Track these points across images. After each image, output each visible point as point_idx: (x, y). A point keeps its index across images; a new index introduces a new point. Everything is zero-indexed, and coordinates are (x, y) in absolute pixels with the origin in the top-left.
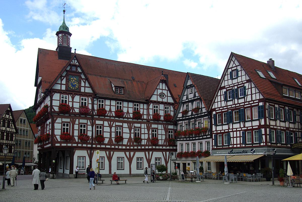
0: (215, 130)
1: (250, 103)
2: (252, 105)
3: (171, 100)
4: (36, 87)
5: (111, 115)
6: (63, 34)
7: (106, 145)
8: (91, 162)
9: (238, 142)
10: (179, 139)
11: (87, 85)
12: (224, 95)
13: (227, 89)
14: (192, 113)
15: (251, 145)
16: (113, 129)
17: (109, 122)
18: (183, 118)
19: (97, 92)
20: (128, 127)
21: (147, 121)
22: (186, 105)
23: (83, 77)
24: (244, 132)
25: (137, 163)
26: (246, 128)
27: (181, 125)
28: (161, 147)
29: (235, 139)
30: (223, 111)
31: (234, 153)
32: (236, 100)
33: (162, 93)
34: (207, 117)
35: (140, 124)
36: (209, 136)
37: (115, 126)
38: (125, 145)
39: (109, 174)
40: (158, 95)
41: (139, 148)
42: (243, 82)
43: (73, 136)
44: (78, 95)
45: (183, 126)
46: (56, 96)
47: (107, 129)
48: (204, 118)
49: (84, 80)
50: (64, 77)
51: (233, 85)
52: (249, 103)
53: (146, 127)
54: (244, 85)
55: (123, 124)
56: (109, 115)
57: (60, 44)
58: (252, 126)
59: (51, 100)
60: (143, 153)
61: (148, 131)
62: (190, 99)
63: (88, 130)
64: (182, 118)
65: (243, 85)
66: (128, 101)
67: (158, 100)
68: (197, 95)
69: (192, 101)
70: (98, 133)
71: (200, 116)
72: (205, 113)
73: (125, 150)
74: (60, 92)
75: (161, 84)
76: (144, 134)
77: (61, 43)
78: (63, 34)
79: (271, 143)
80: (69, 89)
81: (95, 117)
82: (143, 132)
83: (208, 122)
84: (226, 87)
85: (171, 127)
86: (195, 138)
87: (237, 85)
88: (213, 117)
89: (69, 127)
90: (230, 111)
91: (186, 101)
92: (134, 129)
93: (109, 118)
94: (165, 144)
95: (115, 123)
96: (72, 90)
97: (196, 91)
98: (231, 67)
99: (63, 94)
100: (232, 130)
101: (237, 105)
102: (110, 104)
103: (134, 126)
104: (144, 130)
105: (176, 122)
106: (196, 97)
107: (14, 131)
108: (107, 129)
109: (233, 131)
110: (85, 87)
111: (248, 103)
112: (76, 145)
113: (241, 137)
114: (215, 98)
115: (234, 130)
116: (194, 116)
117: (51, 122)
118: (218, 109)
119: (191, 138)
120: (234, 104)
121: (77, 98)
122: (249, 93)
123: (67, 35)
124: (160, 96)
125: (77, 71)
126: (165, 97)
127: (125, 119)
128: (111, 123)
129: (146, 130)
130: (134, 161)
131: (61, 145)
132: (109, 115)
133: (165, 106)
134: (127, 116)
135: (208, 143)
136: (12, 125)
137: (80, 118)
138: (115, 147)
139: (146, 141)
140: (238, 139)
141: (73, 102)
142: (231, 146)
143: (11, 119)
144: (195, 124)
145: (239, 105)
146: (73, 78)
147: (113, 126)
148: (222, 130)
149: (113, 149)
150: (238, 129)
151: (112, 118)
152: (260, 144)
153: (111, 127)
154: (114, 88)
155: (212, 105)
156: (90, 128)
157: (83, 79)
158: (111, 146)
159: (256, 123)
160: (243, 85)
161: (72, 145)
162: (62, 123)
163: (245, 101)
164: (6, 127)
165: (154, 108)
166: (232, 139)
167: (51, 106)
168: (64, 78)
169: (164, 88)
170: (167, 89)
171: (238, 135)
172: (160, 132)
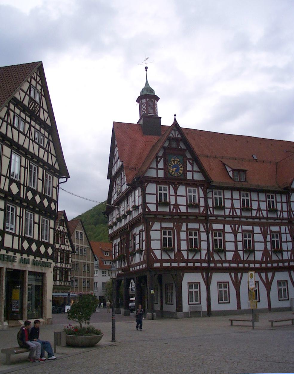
4: (110, 180)
5: (235, 214)
6: (148, 99)
7: (229, 262)
11: (196, 168)
16: (239, 237)
17: (233, 226)
19: (213, 180)
20: (261, 232)
21: (289, 221)
23: (189, 156)
25: (280, 291)
35: (279, 227)
37: (241, 231)
38: (258, 262)
39: (237, 309)
41: (281, 264)
43: (179, 250)
44: (182, 185)
46: (151, 188)
49: (191, 161)
50: (161, 157)
53: (288, 231)
55: (253, 228)
57: (144, 113)
60: (287, 273)
63: (186, 241)
74: (156, 181)
76: (287, 242)
77: (145, 112)
78: (148, 99)
80: (169, 176)
81: (210, 218)
82: (284, 239)
89: (171, 236)
93: (231, 219)
95: (241, 226)
99: (160, 184)
102: (232, 197)
103: (271, 231)
107: (71, 249)
108: (230, 237)
112: (183, 264)
117: (143, 229)
121: (182, 190)
123: (153, 100)
125: (180, 148)
127: (256, 220)
130: (274, 287)
134: (258, 215)
136: (67, 241)
139: (290, 253)
141: (176, 196)
143: (65, 233)
147: (239, 231)
149: (241, 268)
151: (236, 219)
153: (235, 233)
154: (231, 174)
156: (204, 236)
157: (189, 160)
158: (238, 265)
164: (60, 244)
168: (160, 160)
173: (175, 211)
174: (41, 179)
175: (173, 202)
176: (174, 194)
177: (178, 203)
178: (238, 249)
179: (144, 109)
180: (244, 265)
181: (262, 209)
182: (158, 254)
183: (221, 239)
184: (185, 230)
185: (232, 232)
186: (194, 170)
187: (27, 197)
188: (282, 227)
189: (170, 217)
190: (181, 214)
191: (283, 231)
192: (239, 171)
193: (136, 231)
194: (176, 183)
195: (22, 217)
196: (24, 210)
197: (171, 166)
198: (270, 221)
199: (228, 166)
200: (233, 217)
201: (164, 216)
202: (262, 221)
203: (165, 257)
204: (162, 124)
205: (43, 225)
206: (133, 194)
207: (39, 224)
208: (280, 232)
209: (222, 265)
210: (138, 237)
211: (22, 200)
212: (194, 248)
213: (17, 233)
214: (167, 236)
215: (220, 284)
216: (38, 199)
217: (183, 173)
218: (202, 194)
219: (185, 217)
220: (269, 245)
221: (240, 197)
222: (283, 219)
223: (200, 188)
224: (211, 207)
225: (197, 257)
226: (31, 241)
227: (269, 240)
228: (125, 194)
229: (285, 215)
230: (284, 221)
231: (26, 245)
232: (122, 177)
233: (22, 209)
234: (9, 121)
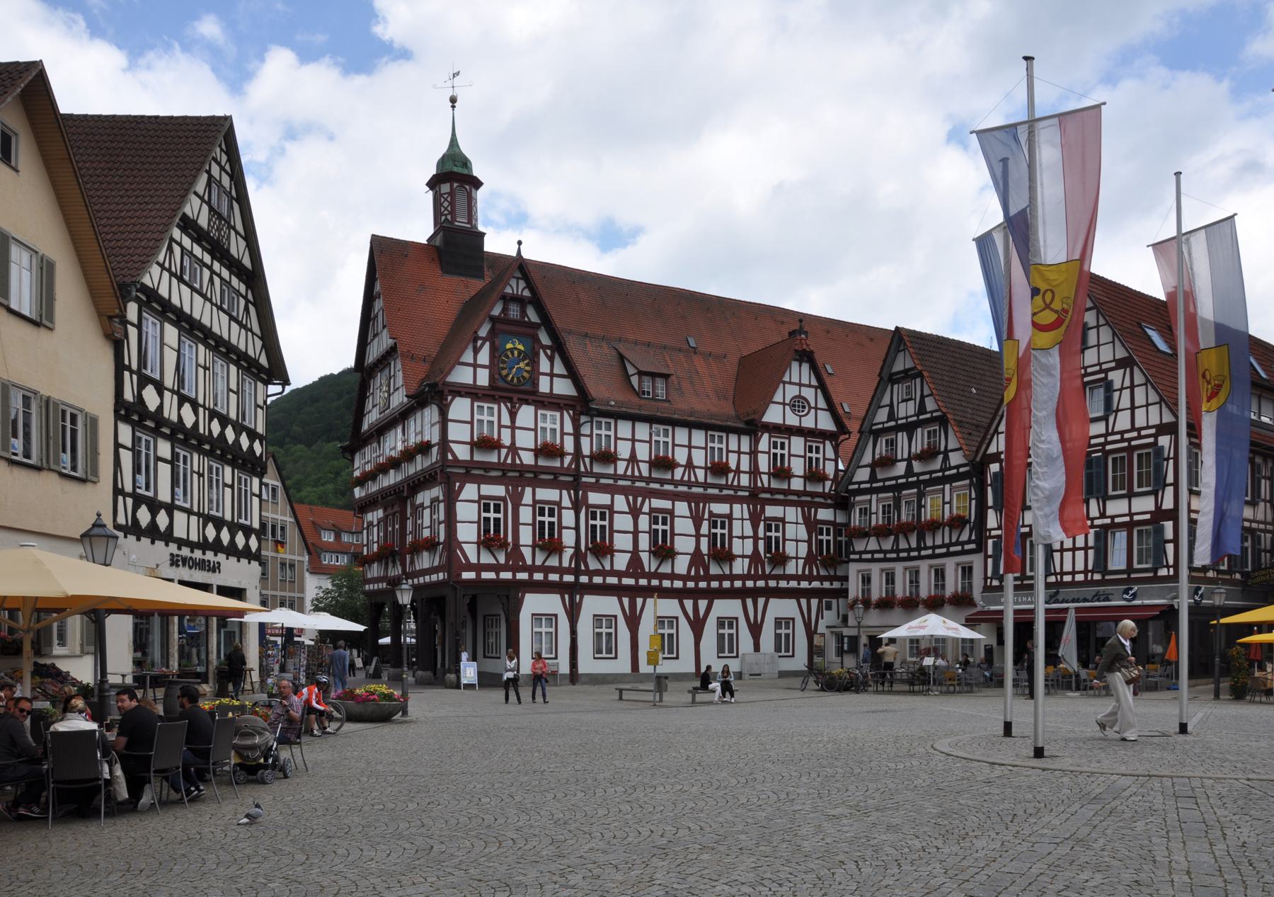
0: (996, 526)
3: (826, 423)
5: (637, 473)
9: (1080, 566)
10: (857, 557)
11: (559, 368)
14: (909, 467)
15: (1125, 576)
16: (644, 522)
17: (631, 498)
18: (874, 485)
19: (594, 397)
22: (887, 441)
24: (1103, 534)
25: (721, 638)
26: (1108, 521)
27: (866, 509)
28: (793, 584)
29: (1068, 555)
33: (800, 396)
34: (967, 482)
35: (728, 506)
38: (679, 577)
39: (630, 672)
40: (787, 404)
41: (726, 584)
43: (517, 545)
44: (528, 404)
45: (874, 510)
46: (460, 408)
47: (623, 522)
48: (954, 484)
53: (746, 515)
56: (629, 473)
58: (1131, 514)
59: (444, 422)
60: (738, 602)
61: (755, 527)
62: (904, 421)
64: (868, 485)
65: (1103, 375)
66: (691, 425)
67: (786, 423)
68: (930, 404)
69: (910, 428)
70: (594, 537)
71: (938, 477)
72: (957, 467)
74: (473, 393)
75: (795, 365)
76: (743, 538)
79: (1219, 572)
80: (501, 384)
81: (584, 479)
82: (737, 531)
83: (971, 499)
85: (824, 514)
88: (989, 482)
89: (501, 516)
91: (886, 425)
92: (709, 520)
93: (629, 483)
94: (807, 572)
95: (647, 500)
96: (509, 386)
97: (926, 392)
103: (710, 512)
104: (742, 527)
105: (847, 499)
106: (926, 413)
108: (623, 522)
111: (1118, 437)
113: (1091, 548)
114: (998, 418)
116: (915, 479)
117: (441, 498)
119: (903, 551)
121: (526, 414)
127: (681, 488)
129: (748, 524)
131: (478, 575)
132: (629, 473)
133: (808, 444)
135: (967, 571)
137: (536, 483)
139: (747, 561)
140: (1080, 555)
141: (513, 427)
144: (920, 506)
146: (513, 343)
151: (638, 484)
152: (1155, 570)
153: (635, 512)
155: (987, 442)
156: (568, 517)
157: (545, 348)
159: (1144, 505)
160: (1103, 375)
161: (514, 576)
162: (478, 502)
165: (773, 451)
167: (444, 443)
169: (805, 381)
170: (814, 382)
172: (791, 531)
173: (509, 461)
174: (235, 390)
175: (506, 440)
176: (509, 424)
177: (517, 445)
180: (649, 582)
181: (696, 463)
182: (471, 552)
183: (605, 526)
184: (530, 502)
186: (556, 371)
188: (734, 506)
189: (498, 473)
190: (523, 469)
191: (737, 514)
192: (653, 375)
193: (424, 497)
194: (515, 400)
195: (203, 475)
196: (206, 459)
197: (504, 362)
198: (710, 491)
199: (629, 361)
200: (633, 479)
201: (486, 470)
202: (695, 490)
203: (486, 559)
204: (485, 249)
205: (240, 489)
206: (419, 415)
207: (232, 487)
208: (730, 517)
209: (604, 580)
210: (427, 512)
211: (201, 440)
212: (549, 543)
213: (195, 509)
214: (492, 515)
215: (598, 619)
216: (230, 434)
217: (530, 377)
218: (569, 427)
219: (531, 475)
220: (704, 542)
221: (651, 434)
222: (739, 488)
223: (565, 412)
225: (553, 562)
226: (219, 523)
227: (707, 533)
228: (399, 414)
229: (745, 480)
230: (740, 493)
231: (211, 532)
232: (392, 374)
233: (201, 457)
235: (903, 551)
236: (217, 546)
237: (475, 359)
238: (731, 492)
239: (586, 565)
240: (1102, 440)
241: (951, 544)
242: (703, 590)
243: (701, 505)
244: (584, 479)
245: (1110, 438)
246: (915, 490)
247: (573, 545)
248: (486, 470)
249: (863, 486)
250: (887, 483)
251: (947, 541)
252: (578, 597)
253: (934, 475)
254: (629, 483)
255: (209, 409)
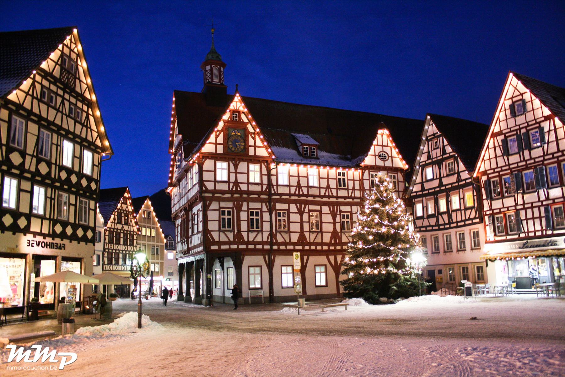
1: (555, 155)
2: (560, 159)
6: (213, 66)
7: (294, 244)
8: (271, 274)
12: (501, 147)
13: (507, 135)
17: (298, 205)
18: (424, 193)
26: (551, 202)
30: (501, 173)
31: (530, 247)
32: (526, 152)
33: (383, 151)
36: (478, 220)
38: (326, 244)
42: (538, 121)
43: (239, 231)
47: (295, 217)
51: (518, 127)
52: (553, 156)
54: (540, 125)
55: (321, 208)
57: (209, 81)
64: (421, 193)
67: (377, 165)
72: (465, 180)
73: (326, 253)
77: (210, 80)
81: (274, 197)
84: (504, 132)
86: (450, 226)
87: (526, 127)
88: (482, 186)
89: (231, 217)
90: (517, 172)
91: (427, 162)
92: (340, 214)
93: (297, 198)
95: (307, 206)
98: (511, 96)
100: (524, 206)
101: (528, 162)
103: (341, 211)
106: (446, 154)
108: (295, 217)
109: (525, 209)
110: (255, 147)
111: (551, 156)
112: (244, 247)
113: (543, 217)
115: (526, 206)
117: (201, 209)
118: (492, 171)
120: (522, 159)
122: (553, 138)
124: (380, 156)
126: (387, 157)
128: (301, 207)
131: (219, 247)
137: (248, 200)
138: (310, 247)
140: (537, 221)
142: (522, 235)
145: (532, 161)
146: (235, 132)
148: (503, 207)
150: (534, 205)
153: (301, 213)
156: (266, 216)
157: (251, 134)
162: (219, 210)
163: (546, 153)
166: (524, 223)
171: (536, 214)
174: (79, 156)
176: (234, 171)
178: (304, 231)
179: (208, 77)
180: (310, 247)
182: (215, 236)
184: (246, 210)
185: (297, 211)
187: (59, 176)
190: (241, 192)
194: (237, 159)
196: (57, 191)
198: (340, 200)
200: (299, 195)
203: (223, 238)
206: (192, 170)
207: (75, 205)
211: (54, 181)
213: (48, 216)
214: (226, 217)
217: (244, 148)
224: (275, 185)
225: (259, 239)
226: (65, 224)
229: (358, 194)
230: (355, 200)
231: (58, 229)
233: (53, 190)
234: (35, 95)
235: (442, 225)
236: (63, 235)
237: (216, 140)
238: (351, 200)
239: (276, 240)
240: (542, 159)
241: (466, 220)
242: (339, 250)
243: (336, 207)
244: (274, 197)
245: (546, 158)
246: (445, 193)
247: (269, 230)
248: (223, 194)
249: (418, 194)
250: (430, 191)
251: (464, 218)
252: (272, 257)
253: (453, 185)
254: (297, 198)
255: (59, 166)
